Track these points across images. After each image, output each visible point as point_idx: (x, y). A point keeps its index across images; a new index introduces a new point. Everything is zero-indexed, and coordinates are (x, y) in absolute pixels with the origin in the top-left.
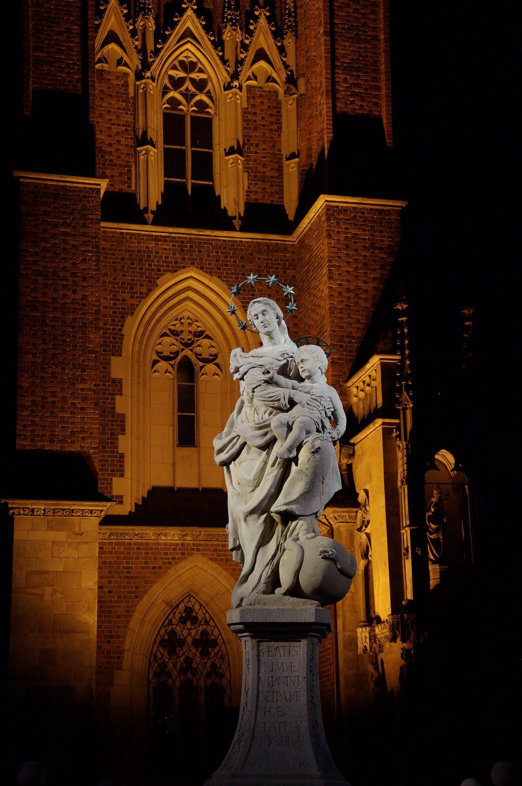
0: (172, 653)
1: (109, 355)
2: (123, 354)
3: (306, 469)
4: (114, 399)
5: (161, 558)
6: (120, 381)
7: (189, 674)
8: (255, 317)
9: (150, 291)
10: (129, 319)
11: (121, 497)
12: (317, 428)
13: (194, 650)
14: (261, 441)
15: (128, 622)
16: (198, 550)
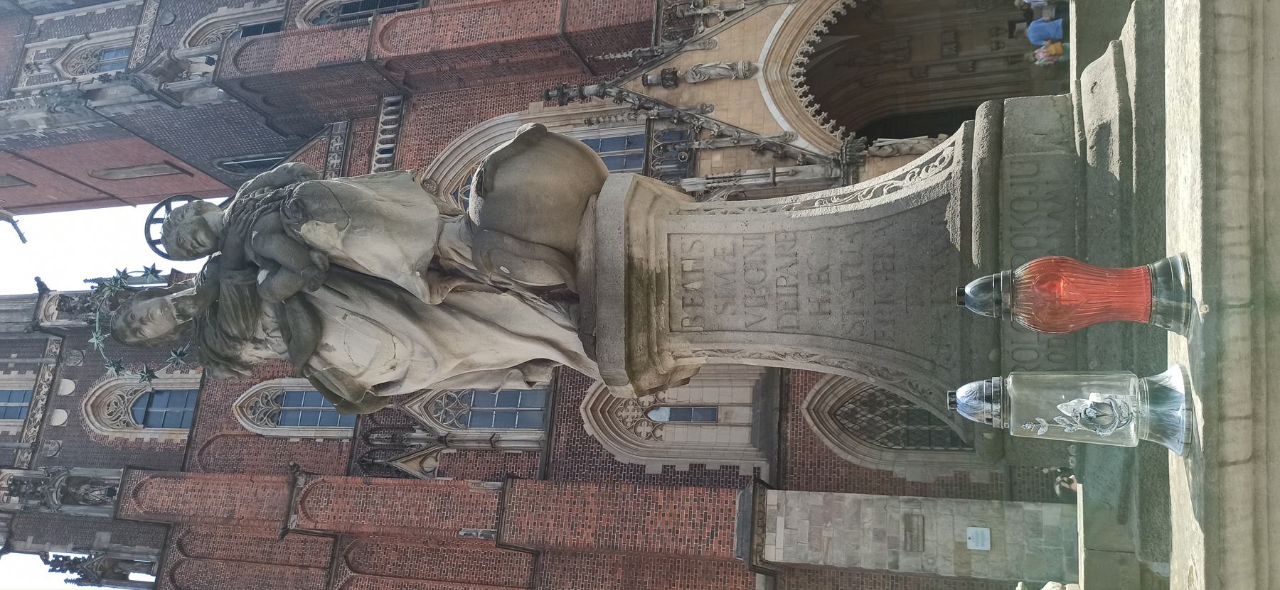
1: (644, 475)
2: (644, 464)
3: (340, 230)
4: (678, 472)
5: (804, 438)
6: (665, 467)
7: (898, 416)
8: (138, 335)
9: (596, 441)
10: (618, 458)
11: (755, 468)
12: (273, 211)
13: (878, 413)
14: (305, 326)
15: (854, 465)
16: (797, 408)
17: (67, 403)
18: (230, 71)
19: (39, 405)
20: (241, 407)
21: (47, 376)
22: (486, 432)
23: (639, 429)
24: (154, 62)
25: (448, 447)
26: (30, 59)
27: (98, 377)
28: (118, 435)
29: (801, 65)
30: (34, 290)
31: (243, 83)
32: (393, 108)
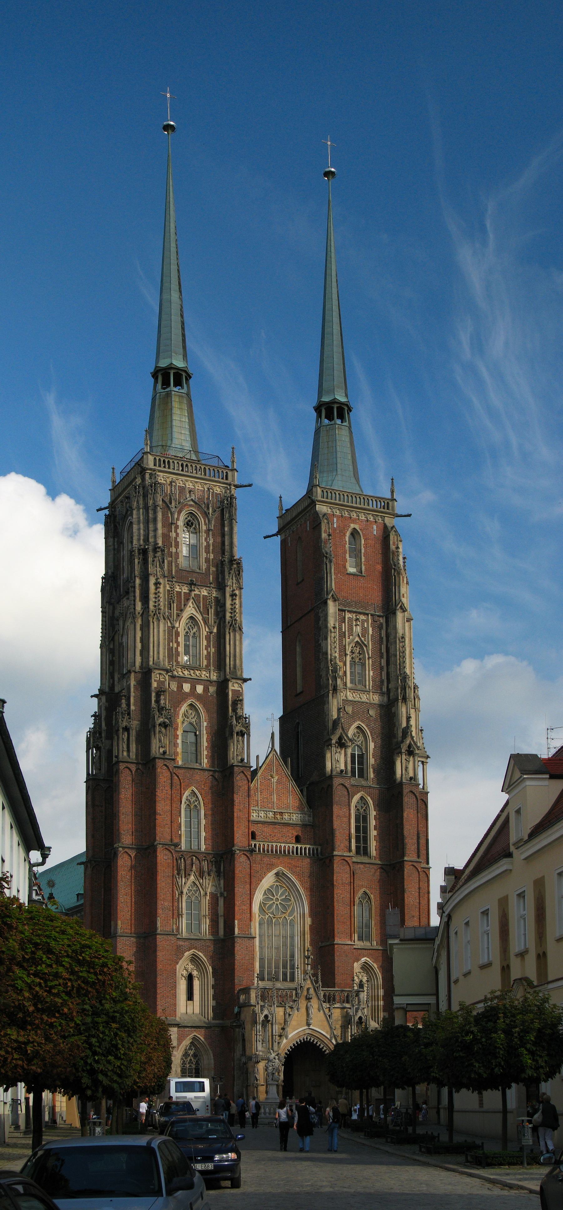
0: (186, 1059)
17: (193, 688)
18: (336, 782)
19: (192, 672)
20: (192, 790)
21: (204, 673)
22: (184, 911)
23: (185, 971)
24: (345, 738)
25: (179, 895)
26: (362, 617)
27: (204, 706)
28: (179, 724)
29: (310, 1039)
30: (245, 676)
31: (330, 786)
32: (315, 852)
